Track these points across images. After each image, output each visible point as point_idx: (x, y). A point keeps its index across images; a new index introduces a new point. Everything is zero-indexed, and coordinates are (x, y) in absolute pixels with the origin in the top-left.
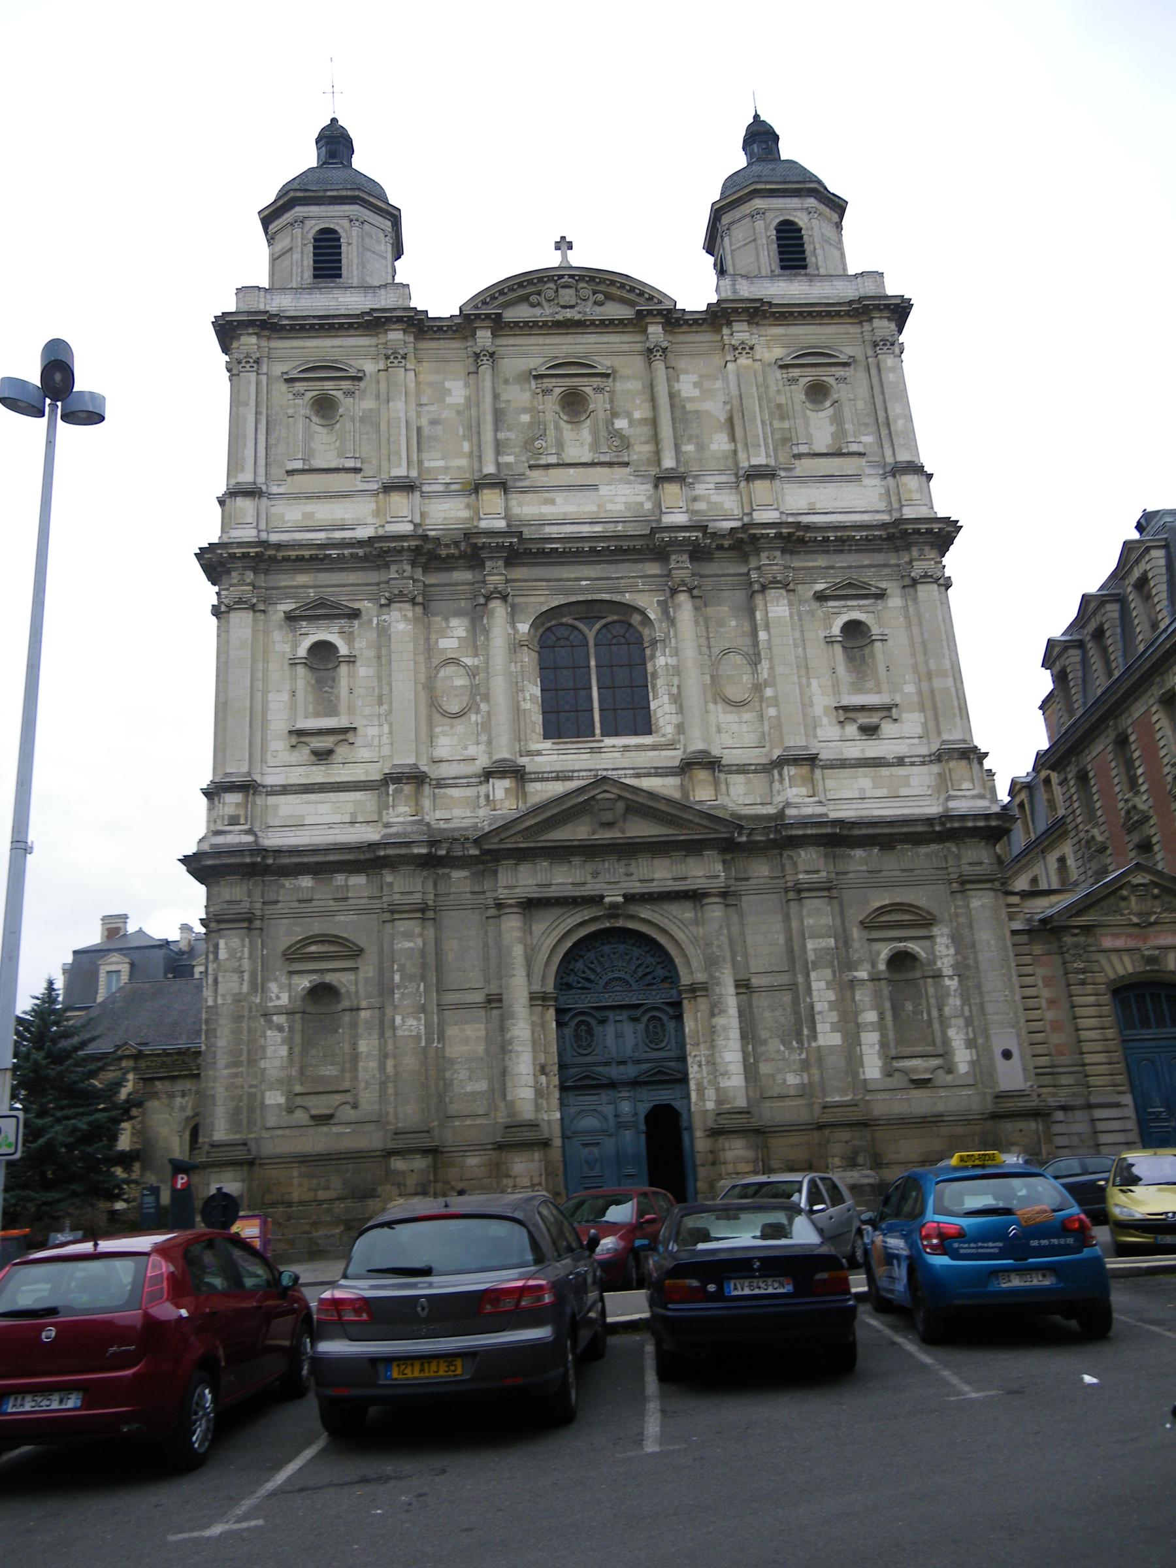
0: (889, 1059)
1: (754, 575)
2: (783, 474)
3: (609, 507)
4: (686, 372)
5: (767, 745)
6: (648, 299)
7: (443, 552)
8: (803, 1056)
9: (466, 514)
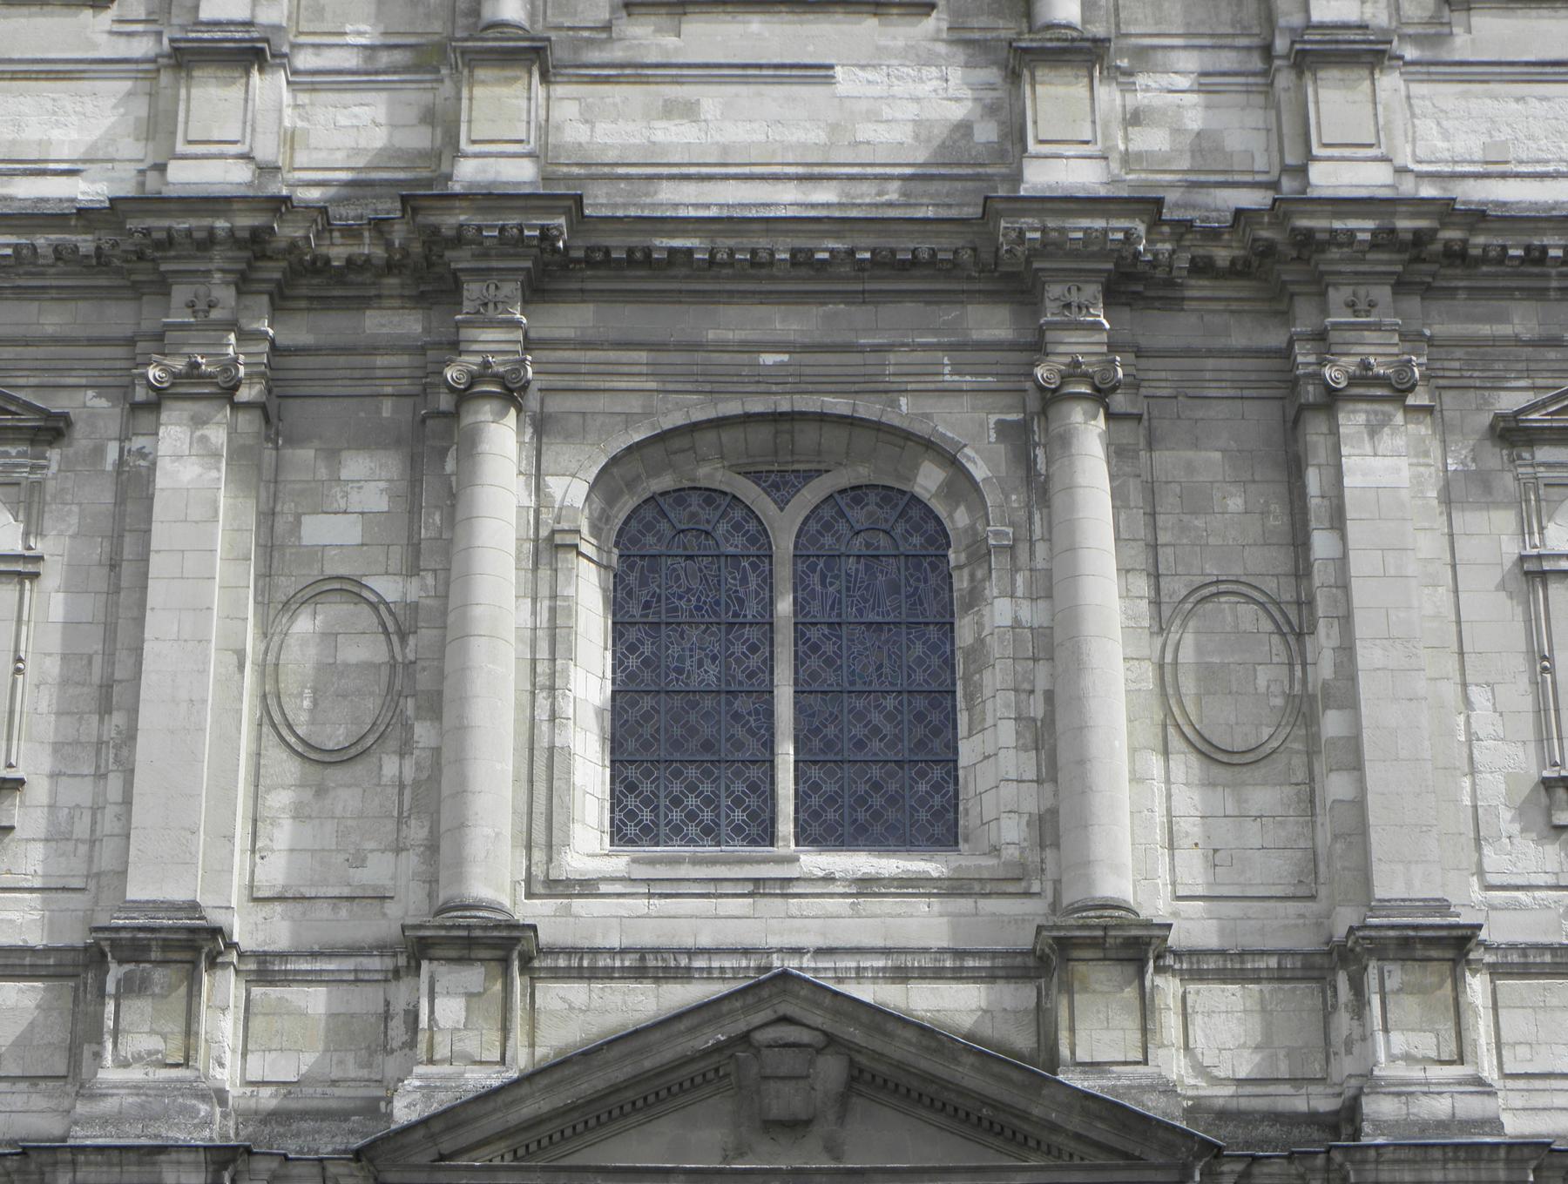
1: (1305, 357)
3: (866, 131)
5: (1323, 892)
7: (338, 252)
9: (419, 139)
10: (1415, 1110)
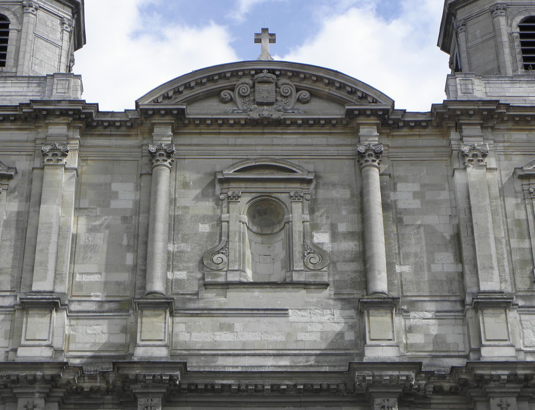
2: (521, 303)
4: (405, 180)
6: (361, 98)
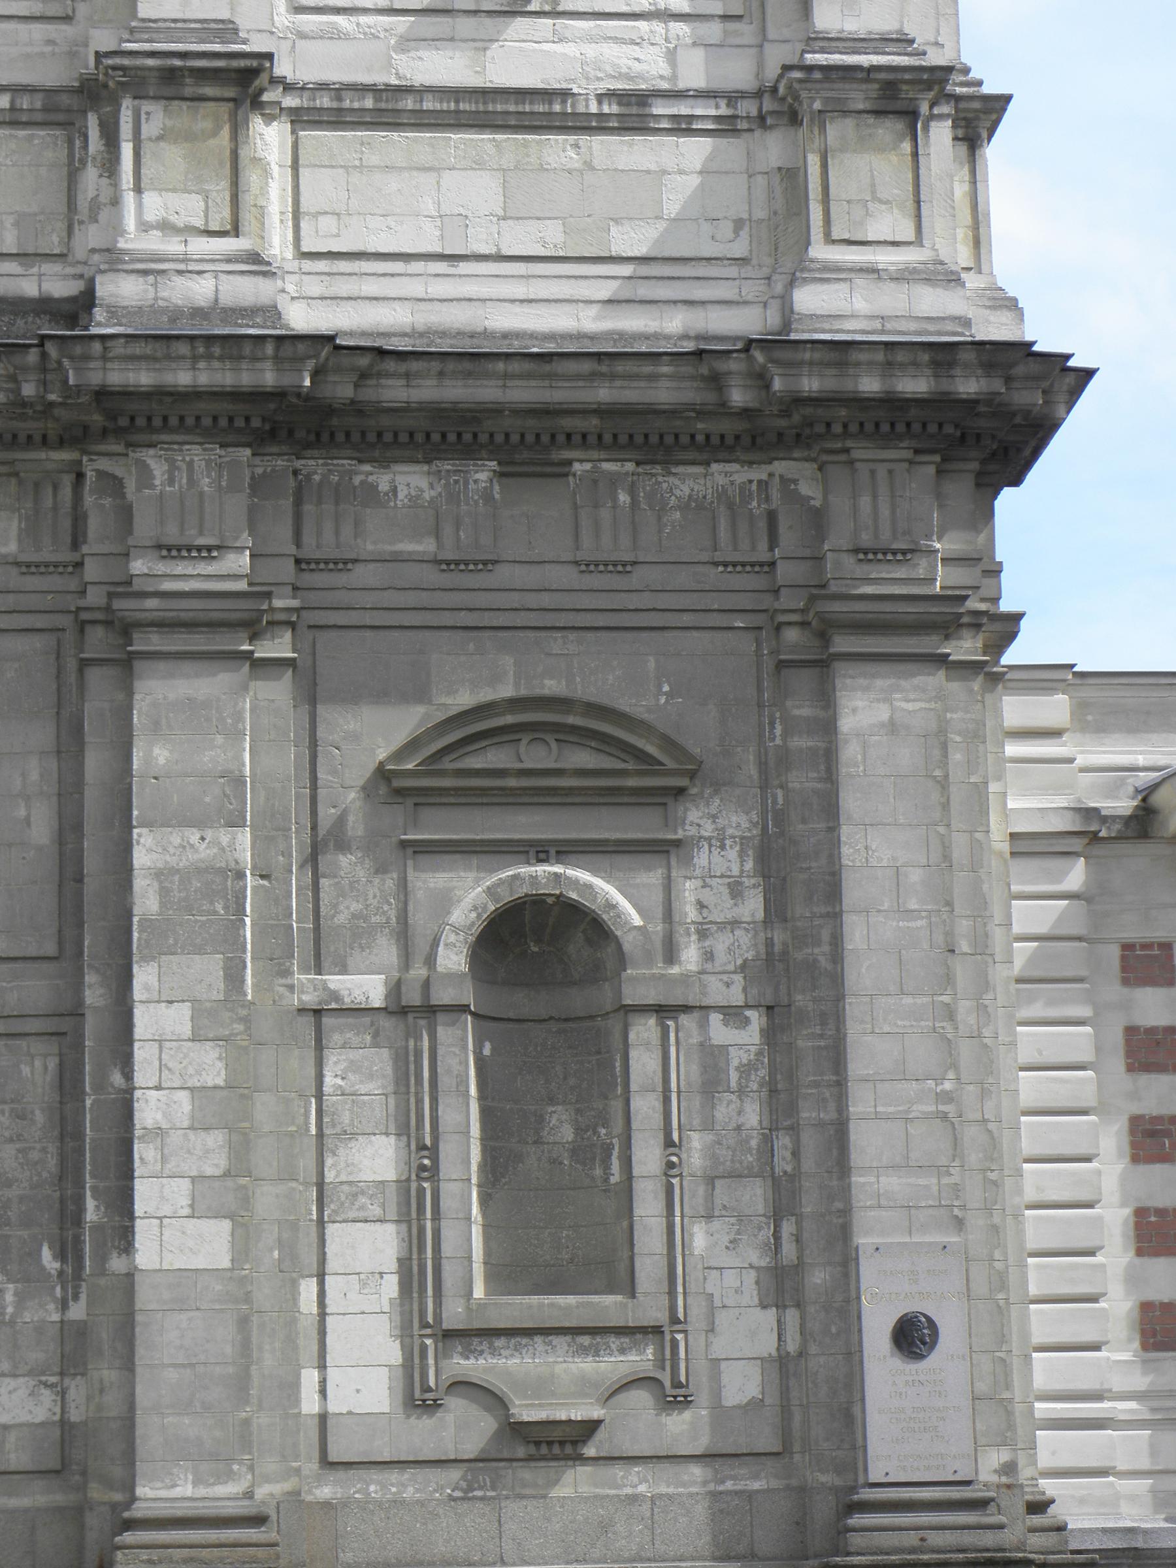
0: (431, 1331)
8: (77, 1311)
10: (165, 294)
